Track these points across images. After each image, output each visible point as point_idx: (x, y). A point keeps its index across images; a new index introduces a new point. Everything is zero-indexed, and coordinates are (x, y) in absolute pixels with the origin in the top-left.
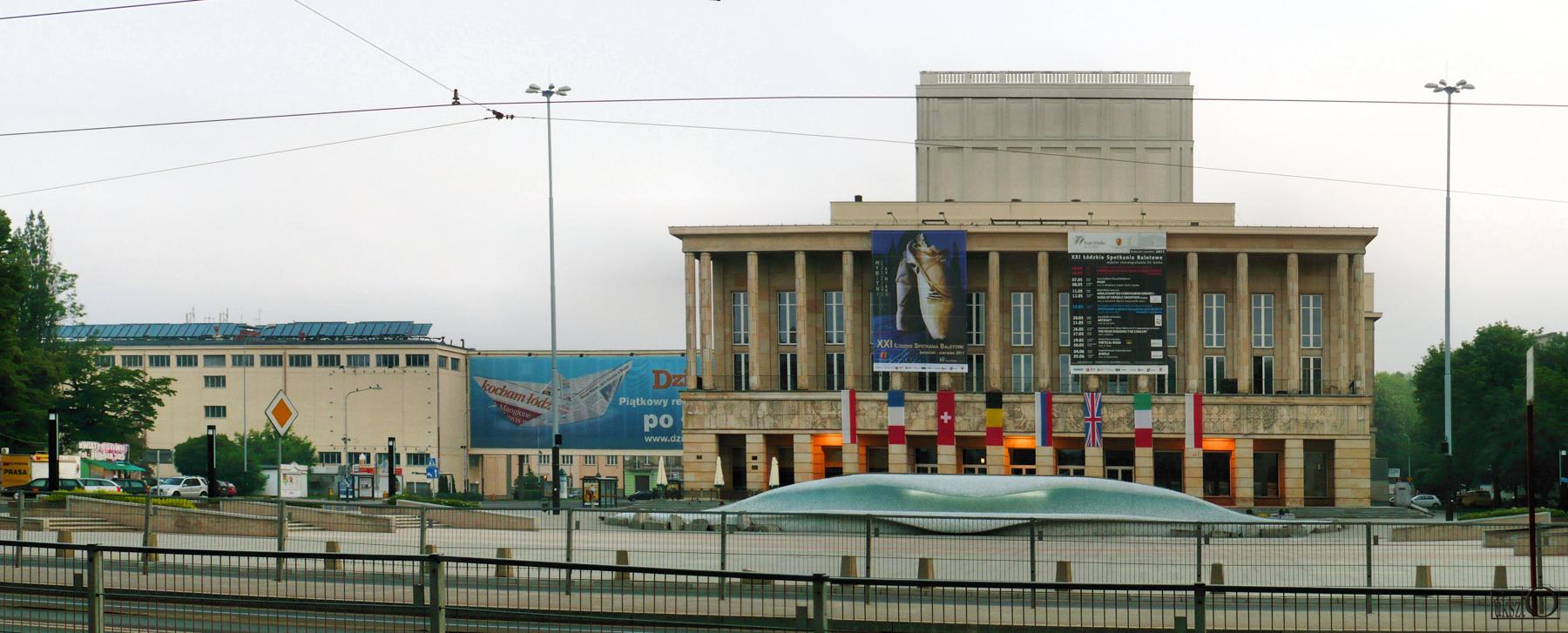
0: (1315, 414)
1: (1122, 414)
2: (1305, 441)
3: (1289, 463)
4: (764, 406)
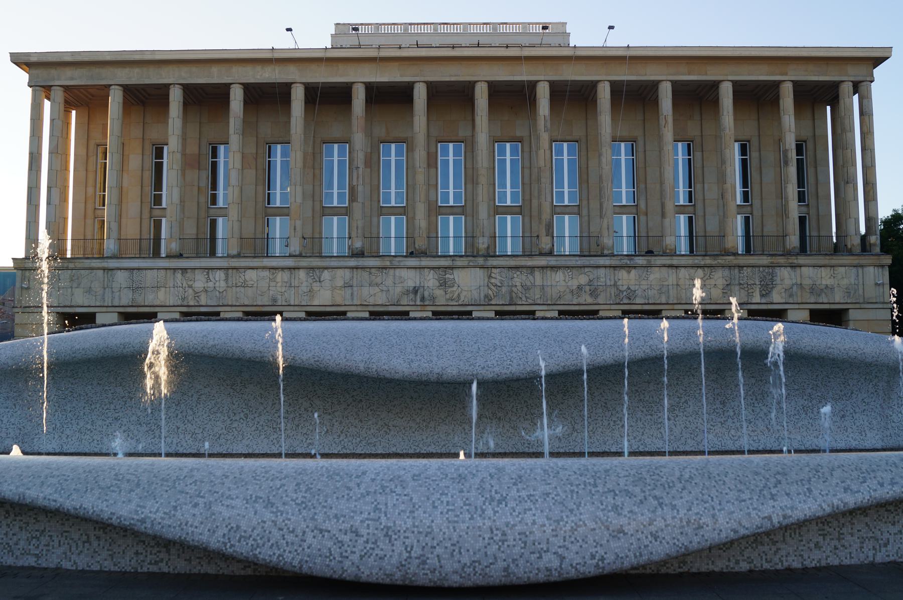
0: (824, 277)
1: (583, 280)
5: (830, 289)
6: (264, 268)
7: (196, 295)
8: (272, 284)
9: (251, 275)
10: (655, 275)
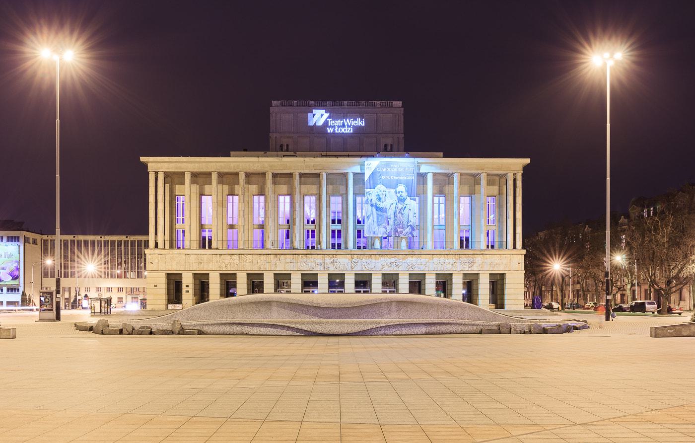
0: (496, 260)
2: (490, 274)
3: (481, 286)
7: (226, 266)
8: (259, 261)
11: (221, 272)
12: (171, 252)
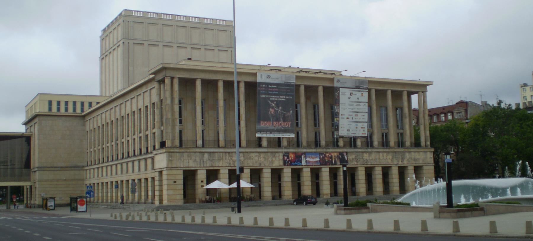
0: (417, 156)
1: (354, 156)
4: (206, 155)
5: (418, 159)
6: (256, 152)
9: (253, 155)
10: (373, 156)
11: (230, 168)
12: (188, 151)
